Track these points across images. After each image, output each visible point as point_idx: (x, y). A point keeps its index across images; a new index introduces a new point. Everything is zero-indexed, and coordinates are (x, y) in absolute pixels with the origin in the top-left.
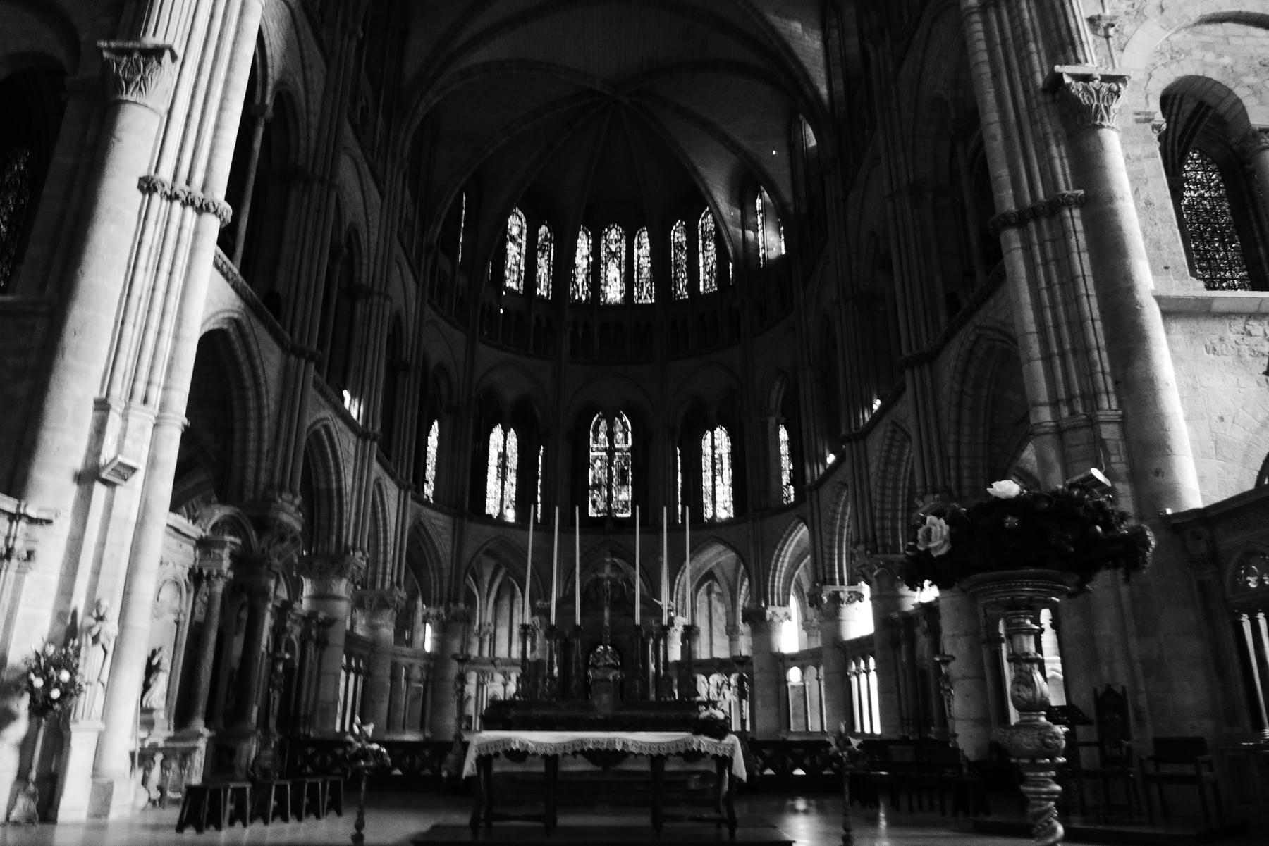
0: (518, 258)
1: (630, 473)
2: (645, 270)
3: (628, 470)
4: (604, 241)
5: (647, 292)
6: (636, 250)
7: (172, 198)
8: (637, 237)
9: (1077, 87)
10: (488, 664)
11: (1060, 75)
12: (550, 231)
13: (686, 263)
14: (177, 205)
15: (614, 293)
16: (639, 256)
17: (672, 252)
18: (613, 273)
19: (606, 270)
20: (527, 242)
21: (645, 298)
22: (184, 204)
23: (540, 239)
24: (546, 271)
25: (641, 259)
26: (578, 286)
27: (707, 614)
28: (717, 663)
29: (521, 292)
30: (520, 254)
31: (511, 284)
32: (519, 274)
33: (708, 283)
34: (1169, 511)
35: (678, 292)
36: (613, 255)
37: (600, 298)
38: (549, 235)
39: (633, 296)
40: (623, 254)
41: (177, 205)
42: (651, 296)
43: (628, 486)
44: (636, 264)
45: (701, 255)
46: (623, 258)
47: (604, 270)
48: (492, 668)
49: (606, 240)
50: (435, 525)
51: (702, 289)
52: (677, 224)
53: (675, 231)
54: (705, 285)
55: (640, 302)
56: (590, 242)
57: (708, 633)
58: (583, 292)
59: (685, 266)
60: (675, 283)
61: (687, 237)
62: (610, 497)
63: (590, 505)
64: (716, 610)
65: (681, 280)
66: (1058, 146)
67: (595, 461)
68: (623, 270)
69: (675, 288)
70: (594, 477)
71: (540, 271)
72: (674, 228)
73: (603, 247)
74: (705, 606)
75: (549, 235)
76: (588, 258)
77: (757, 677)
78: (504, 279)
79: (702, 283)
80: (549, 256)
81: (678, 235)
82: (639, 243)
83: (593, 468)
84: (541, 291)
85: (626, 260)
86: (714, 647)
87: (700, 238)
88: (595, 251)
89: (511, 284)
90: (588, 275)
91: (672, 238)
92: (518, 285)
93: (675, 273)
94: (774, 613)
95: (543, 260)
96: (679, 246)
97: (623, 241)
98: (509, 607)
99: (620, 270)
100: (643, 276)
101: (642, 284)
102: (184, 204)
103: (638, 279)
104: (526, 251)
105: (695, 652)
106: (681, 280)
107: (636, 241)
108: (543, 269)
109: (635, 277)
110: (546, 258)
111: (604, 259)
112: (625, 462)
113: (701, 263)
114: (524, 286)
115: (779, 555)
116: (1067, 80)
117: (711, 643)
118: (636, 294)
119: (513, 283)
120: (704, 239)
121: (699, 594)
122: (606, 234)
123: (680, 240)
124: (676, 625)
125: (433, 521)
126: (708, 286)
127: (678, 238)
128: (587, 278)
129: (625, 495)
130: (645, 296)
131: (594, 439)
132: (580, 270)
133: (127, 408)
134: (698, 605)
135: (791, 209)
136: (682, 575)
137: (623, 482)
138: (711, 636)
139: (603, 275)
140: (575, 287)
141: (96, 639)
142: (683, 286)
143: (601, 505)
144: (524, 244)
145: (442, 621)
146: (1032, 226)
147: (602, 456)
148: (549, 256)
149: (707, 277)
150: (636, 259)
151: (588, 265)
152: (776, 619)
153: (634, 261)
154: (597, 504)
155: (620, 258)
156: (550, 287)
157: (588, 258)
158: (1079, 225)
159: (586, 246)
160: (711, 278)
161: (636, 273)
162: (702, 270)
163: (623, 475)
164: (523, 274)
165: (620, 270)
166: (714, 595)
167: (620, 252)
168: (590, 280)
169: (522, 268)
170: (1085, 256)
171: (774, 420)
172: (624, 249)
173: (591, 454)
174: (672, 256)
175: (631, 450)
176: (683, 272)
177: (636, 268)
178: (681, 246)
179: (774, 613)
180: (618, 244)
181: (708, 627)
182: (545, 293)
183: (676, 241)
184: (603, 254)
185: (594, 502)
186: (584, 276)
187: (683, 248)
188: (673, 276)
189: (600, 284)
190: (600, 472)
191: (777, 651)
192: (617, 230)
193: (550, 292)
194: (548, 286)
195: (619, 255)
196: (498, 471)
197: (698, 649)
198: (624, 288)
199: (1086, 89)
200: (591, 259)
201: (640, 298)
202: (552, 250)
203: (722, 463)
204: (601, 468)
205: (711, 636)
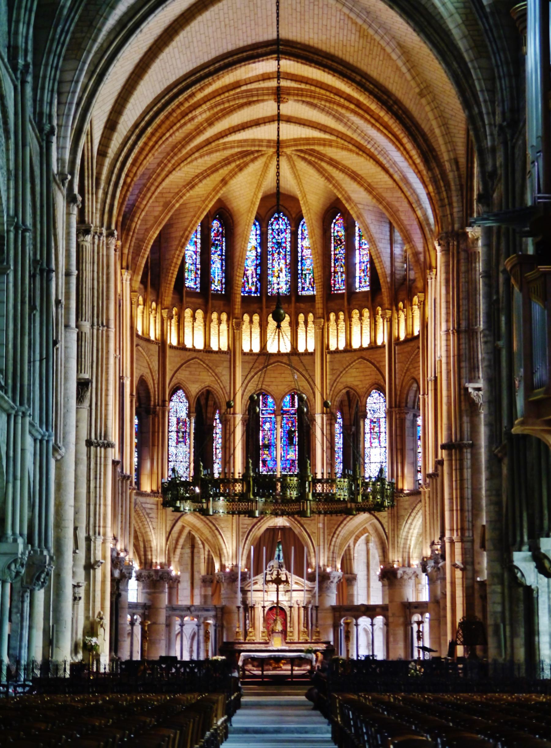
0: (194, 257)
1: (297, 434)
2: (308, 262)
3: (295, 431)
4: (270, 231)
5: (310, 284)
6: (299, 240)
7: (96, 447)
8: (300, 227)
9: (473, 393)
10: (185, 611)
11: (467, 389)
12: (221, 226)
13: (344, 258)
14: (99, 448)
16: (302, 246)
17: (332, 245)
19: (273, 260)
20: (201, 239)
21: (308, 289)
22: (101, 447)
23: (213, 234)
24: (219, 266)
25: (305, 250)
26: (247, 277)
27: (366, 561)
28: (363, 609)
29: (198, 290)
30: (195, 253)
32: (196, 273)
33: (363, 280)
34: (478, 579)
35: (337, 286)
36: (279, 244)
37: (267, 289)
38: (220, 229)
39: (297, 287)
40: (288, 245)
41: (99, 448)
42: (313, 287)
43: (295, 445)
44: (300, 255)
45: (357, 252)
46: (288, 249)
47: (271, 261)
48: (188, 613)
49: (273, 230)
50: (144, 508)
51: (357, 285)
52: (337, 217)
53: (335, 223)
54: (360, 282)
55: (304, 293)
56: (258, 232)
57: (366, 577)
58: (253, 282)
59: (343, 261)
60: (335, 277)
61: (345, 231)
63: (261, 465)
64: (374, 557)
65: (339, 273)
66: (467, 416)
67: (264, 423)
68: (288, 261)
69: (335, 281)
70: (264, 438)
71: (213, 266)
72: (334, 221)
73: (270, 237)
74: (364, 553)
75: (220, 229)
76: (256, 248)
77: (391, 620)
79: (357, 280)
80: (222, 250)
82: (302, 234)
83: (264, 430)
84: (216, 286)
85: (291, 251)
86: (371, 589)
87: (357, 234)
88: (263, 243)
90: (257, 265)
91: (332, 231)
92: (196, 284)
93: (335, 267)
94: (404, 572)
95: (216, 255)
96: (338, 241)
97: (288, 231)
98: (190, 555)
99: (286, 262)
100: (306, 267)
101: (305, 275)
102: (101, 447)
103: (302, 270)
104: (201, 248)
105: (352, 596)
106: (339, 273)
107: (300, 232)
109: (299, 268)
110: (219, 253)
111: (270, 249)
112: (292, 424)
113: (357, 261)
114: (201, 283)
115: (409, 529)
116: (470, 390)
117: (368, 586)
118: (300, 285)
120: (360, 236)
121: (357, 545)
122: (272, 224)
123: (340, 234)
124: (332, 579)
125: (144, 505)
126: (363, 284)
127: (338, 232)
128: (256, 269)
131: (263, 403)
132: (249, 262)
133: (95, 538)
134: (356, 555)
135: (422, 257)
136: (337, 538)
138: (368, 580)
139: (270, 266)
140: (245, 279)
141: (102, 626)
142: (342, 281)
144: (199, 241)
145: (152, 580)
146: (453, 451)
147: (271, 418)
148: (222, 250)
149: (362, 274)
150: (300, 250)
151: (256, 256)
152: (405, 577)
153: (298, 252)
154: (268, 462)
155: (285, 248)
156: (224, 280)
157: (256, 248)
158: (469, 456)
159: (254, 237)
160: (365, 276)
161: (300, 264)
162: (357, 266)
163: (289, 435)
164: (199, 272)
165: (286, 262)
166: (371, 545)
167: (285, 242)
168: (259, 272)
169: (199, 266)
170: (469, 470)
171: (412, 415)
172: (288, 240)
173: (261, 416)
174: (332, 249)
176: (342, 267)
177: (300, 259)
178: (340, 240)
179: (404, 572)
180: (284, 234)
181: (365, 573)
182: (219, 288)
183: (336, 234)
184: (270, 244)
185: (264, 462)
186: (253, 268)
187: (341, 243)
188: (333, 269)
189: (268, 275)
190: (269, 434)
191: (406, 600)
192: (284, 220)
193: (224, 286)
194: (222, 280)
195: (284, 245)
196: (178, 436)
197: (355, 593)
198: (288, 278)
199: (478, 395)
200: (259, 250)
201: (303, 289)
202: (224, 245)
203: (379, 427)
204: (270, 430)
205: (368, 580)
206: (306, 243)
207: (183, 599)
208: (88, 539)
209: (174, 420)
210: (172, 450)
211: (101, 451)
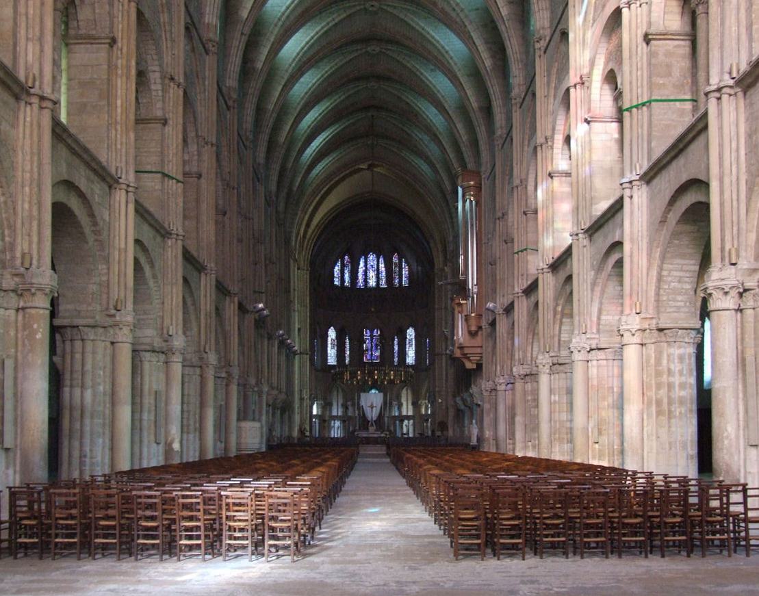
15: (372, 282)
18: (372, 274)
31: (336, 283)
36: (372, 266)
62: (372, 354)
78: (334, 281)
81: (395, 260)
84: (347, 284)
89: (336, 283)
108: (347, 276)
119: (337, 282)
129: (377, 354)
130: (383, 284)
137: (376, 349)
143: (369, 358)
163: (376, 345)
175: (380, 335)
206: (383, 265)
207: (334, 413)
208: (301, 390)
209: (329, 339)
210: (329, 352)
211: (305, 356)
